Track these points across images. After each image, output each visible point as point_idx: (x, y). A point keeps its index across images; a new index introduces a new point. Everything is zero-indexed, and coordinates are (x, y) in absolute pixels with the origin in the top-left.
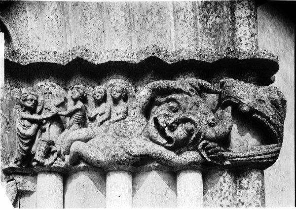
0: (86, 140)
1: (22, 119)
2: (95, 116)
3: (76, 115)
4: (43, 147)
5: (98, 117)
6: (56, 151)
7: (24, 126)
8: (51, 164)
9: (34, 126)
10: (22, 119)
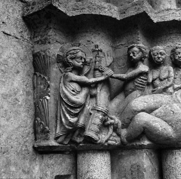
0: (150, 111)
1: (72, 81)
2: (154, 80)
3: (140, 80)
4: (97, 119)
5: (157, 82)
6: (111, 124)
7: (73, 91)
8: (107, 141)
9: (85, 91)
10: (72, 81)
